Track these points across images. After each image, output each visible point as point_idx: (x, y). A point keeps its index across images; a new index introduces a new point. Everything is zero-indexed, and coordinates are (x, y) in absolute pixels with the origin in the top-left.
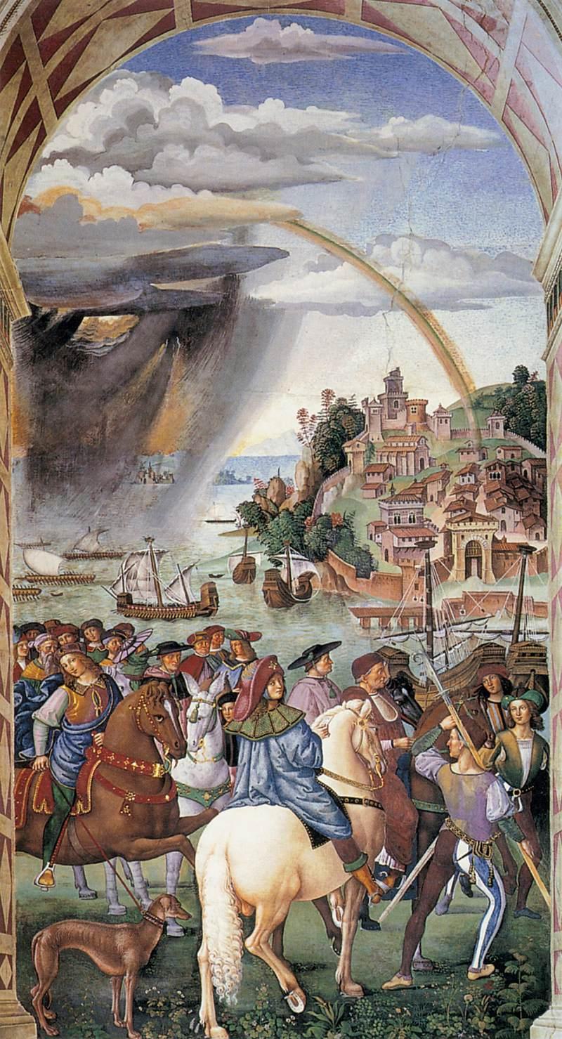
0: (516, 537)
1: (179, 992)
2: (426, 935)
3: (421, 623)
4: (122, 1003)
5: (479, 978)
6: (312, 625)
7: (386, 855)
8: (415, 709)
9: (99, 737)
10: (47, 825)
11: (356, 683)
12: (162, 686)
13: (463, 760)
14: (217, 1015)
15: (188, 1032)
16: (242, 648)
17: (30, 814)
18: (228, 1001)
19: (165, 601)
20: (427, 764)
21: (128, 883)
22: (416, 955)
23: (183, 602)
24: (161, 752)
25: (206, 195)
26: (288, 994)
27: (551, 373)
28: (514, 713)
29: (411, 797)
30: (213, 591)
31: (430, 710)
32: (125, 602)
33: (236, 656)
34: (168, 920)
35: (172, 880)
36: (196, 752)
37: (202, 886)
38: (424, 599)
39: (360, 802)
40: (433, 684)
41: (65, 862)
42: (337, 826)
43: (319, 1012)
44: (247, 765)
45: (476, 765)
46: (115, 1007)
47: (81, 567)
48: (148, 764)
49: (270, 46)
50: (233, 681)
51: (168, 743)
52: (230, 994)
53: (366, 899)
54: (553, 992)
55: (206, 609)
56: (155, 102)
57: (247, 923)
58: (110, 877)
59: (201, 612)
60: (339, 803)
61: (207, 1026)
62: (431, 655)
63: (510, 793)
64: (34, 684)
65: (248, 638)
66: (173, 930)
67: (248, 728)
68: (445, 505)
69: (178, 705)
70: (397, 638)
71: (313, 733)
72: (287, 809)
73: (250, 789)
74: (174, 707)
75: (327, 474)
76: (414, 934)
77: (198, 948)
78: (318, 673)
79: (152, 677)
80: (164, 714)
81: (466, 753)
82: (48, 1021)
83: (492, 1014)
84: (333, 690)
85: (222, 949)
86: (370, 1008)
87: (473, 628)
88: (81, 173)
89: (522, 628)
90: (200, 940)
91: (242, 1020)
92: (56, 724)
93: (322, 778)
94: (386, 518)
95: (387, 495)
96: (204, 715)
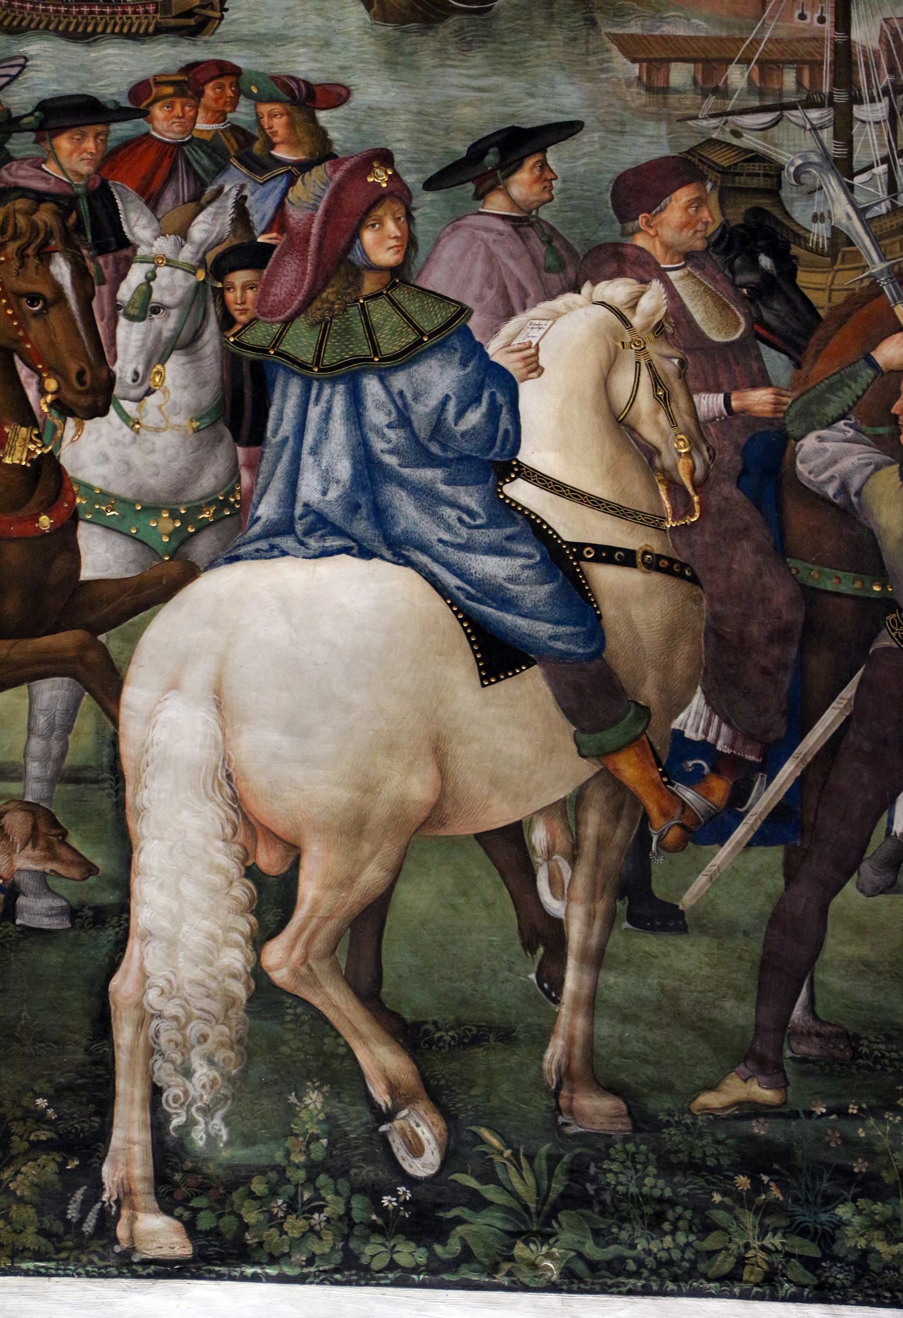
1: (41, 1102)
2: (826, 955)
3: (816, 80)
6: (495, 73)
7: (705, 712)
8: (794, 308)
11: (624, 234)
12: (45, 216)
15: (58, 1227)
16: (291, 125)
18: (198, 1137)
20: (834, 462)
22: (797, 1012)
24: (32, 393)
26: (389, 1116)
33: (273, 146)
34: (26, 881)
35: (45, 758)
36: (139, 400)
37: (138, 780)
38: (829, 18)
39: (627, 559)
40: (851, 244)
42: (558, 623)
43: (488, 1176)
44: (291, 443)
51: (58, 372)
52: (208, 1111)
53: (643, 838)
55: (188, 14)
59: (173, 22)
61: (125, 1213)
69: (90, 264)
70: (749, 120)
71: (495, 365)
72: (408, 573)
73: (299, 510)
74: (80, 273)
77: (113, 967)
78: (513, 202)
79: (17, 188)
80: (47, 292)
84: (554, 251)
86: (652, 1170)
91: (235, 1196)
96: (167, 300)
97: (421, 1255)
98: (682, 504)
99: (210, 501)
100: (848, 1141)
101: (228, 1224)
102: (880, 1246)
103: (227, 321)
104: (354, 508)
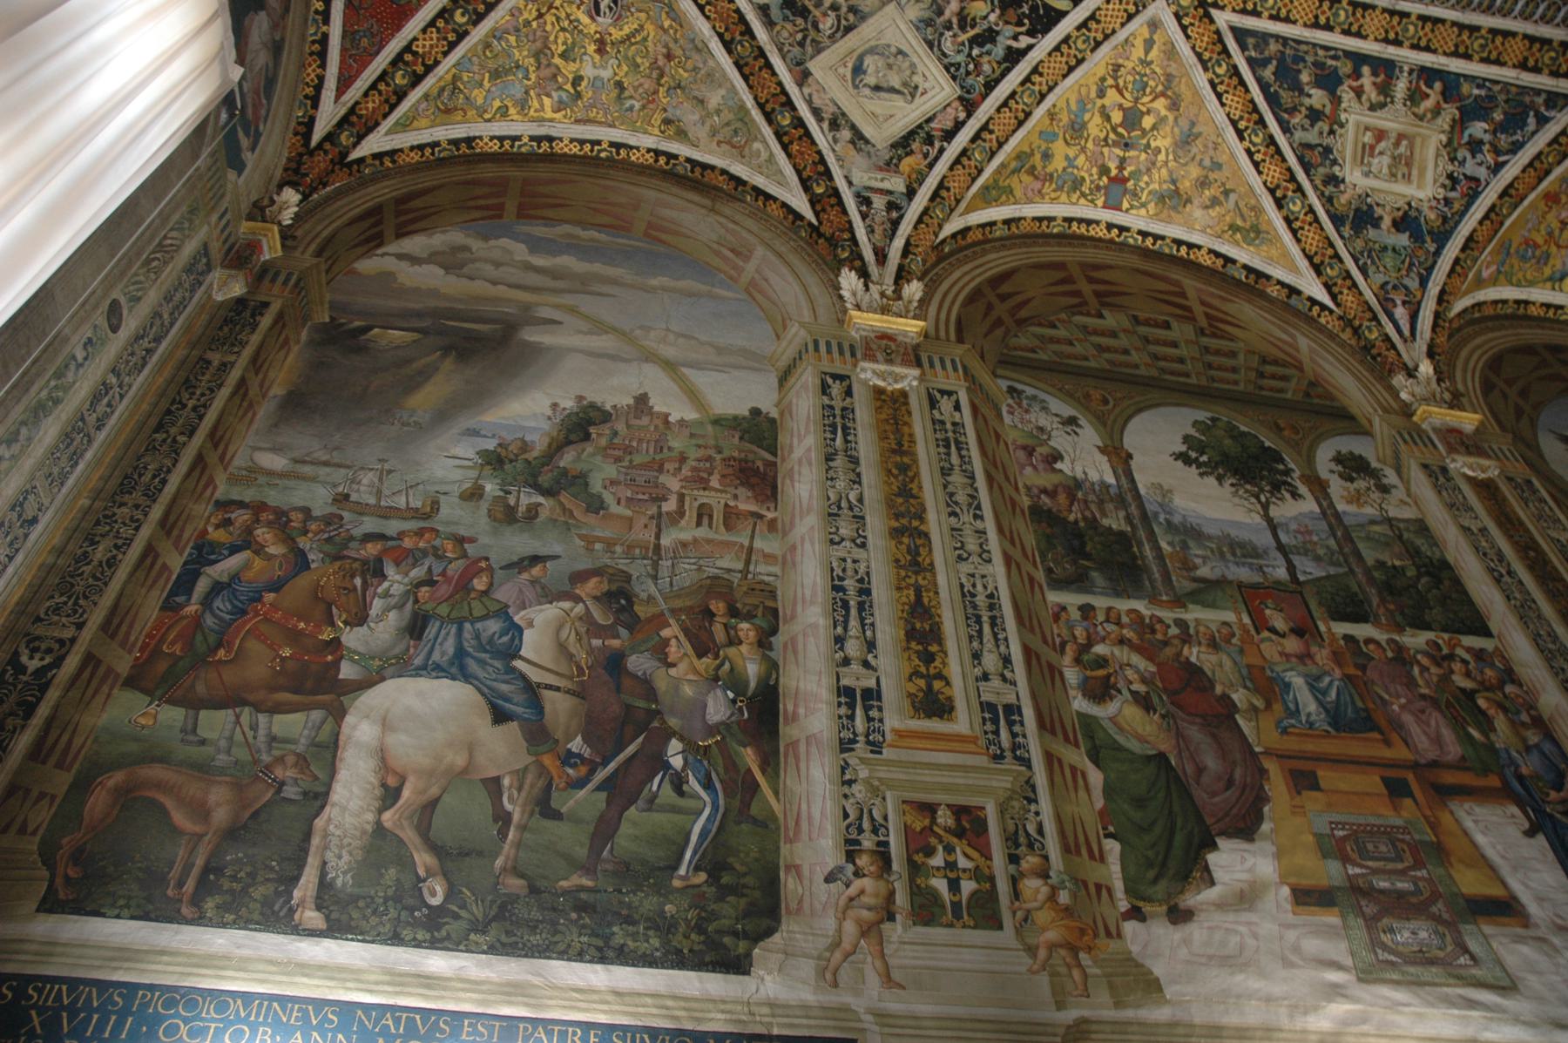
4: (188, 867)
5: (687, 887)
9: (269, 597)
12: (356, 565)
17: (156, 653)
18: (339, 882)
19: (383, 503)
21: (250, 734)
25: (500, 287)
26: (424, 881)
27: (782, 414)
28: (741, 634)
29: (618, 689)
31: (649, 620)
34: (289, 781)
39: (558, 689)
43: (463, 906)
45: (696, 672)
46: (174, 874)
47: (307, 469)
48: (318, 626)
49: (570, 236)
50: (437, 569)
51: (348, 612)
52: (345, 873)
53: (549, 786)
54: (783, 911)
56: (476, 245)
57: (390, 795)
58: (229, 727)
60: (532, 691)
62: (655, 578)
63: (734, 701)
65: (460, 541)
66: (290, 792)
67: (443, 610)
74: (365, 583)
75: (569, 443)
76: (605, 830)
77: (317, 815)
81: (686, 660)
83: (700, 929)
85: (349, 820)
88: (404, 265)
89: (752, 568)
90: (323, 807)
93: (518, 664)
94: (622, 478)
95: (626, 463)
97: (428, 936)
98: (581, 671)
99: (396, 657)
100: (621, 902)
101: (344, 918)
102: (630, 943)
103: (416, 601)
104: (452, 664)
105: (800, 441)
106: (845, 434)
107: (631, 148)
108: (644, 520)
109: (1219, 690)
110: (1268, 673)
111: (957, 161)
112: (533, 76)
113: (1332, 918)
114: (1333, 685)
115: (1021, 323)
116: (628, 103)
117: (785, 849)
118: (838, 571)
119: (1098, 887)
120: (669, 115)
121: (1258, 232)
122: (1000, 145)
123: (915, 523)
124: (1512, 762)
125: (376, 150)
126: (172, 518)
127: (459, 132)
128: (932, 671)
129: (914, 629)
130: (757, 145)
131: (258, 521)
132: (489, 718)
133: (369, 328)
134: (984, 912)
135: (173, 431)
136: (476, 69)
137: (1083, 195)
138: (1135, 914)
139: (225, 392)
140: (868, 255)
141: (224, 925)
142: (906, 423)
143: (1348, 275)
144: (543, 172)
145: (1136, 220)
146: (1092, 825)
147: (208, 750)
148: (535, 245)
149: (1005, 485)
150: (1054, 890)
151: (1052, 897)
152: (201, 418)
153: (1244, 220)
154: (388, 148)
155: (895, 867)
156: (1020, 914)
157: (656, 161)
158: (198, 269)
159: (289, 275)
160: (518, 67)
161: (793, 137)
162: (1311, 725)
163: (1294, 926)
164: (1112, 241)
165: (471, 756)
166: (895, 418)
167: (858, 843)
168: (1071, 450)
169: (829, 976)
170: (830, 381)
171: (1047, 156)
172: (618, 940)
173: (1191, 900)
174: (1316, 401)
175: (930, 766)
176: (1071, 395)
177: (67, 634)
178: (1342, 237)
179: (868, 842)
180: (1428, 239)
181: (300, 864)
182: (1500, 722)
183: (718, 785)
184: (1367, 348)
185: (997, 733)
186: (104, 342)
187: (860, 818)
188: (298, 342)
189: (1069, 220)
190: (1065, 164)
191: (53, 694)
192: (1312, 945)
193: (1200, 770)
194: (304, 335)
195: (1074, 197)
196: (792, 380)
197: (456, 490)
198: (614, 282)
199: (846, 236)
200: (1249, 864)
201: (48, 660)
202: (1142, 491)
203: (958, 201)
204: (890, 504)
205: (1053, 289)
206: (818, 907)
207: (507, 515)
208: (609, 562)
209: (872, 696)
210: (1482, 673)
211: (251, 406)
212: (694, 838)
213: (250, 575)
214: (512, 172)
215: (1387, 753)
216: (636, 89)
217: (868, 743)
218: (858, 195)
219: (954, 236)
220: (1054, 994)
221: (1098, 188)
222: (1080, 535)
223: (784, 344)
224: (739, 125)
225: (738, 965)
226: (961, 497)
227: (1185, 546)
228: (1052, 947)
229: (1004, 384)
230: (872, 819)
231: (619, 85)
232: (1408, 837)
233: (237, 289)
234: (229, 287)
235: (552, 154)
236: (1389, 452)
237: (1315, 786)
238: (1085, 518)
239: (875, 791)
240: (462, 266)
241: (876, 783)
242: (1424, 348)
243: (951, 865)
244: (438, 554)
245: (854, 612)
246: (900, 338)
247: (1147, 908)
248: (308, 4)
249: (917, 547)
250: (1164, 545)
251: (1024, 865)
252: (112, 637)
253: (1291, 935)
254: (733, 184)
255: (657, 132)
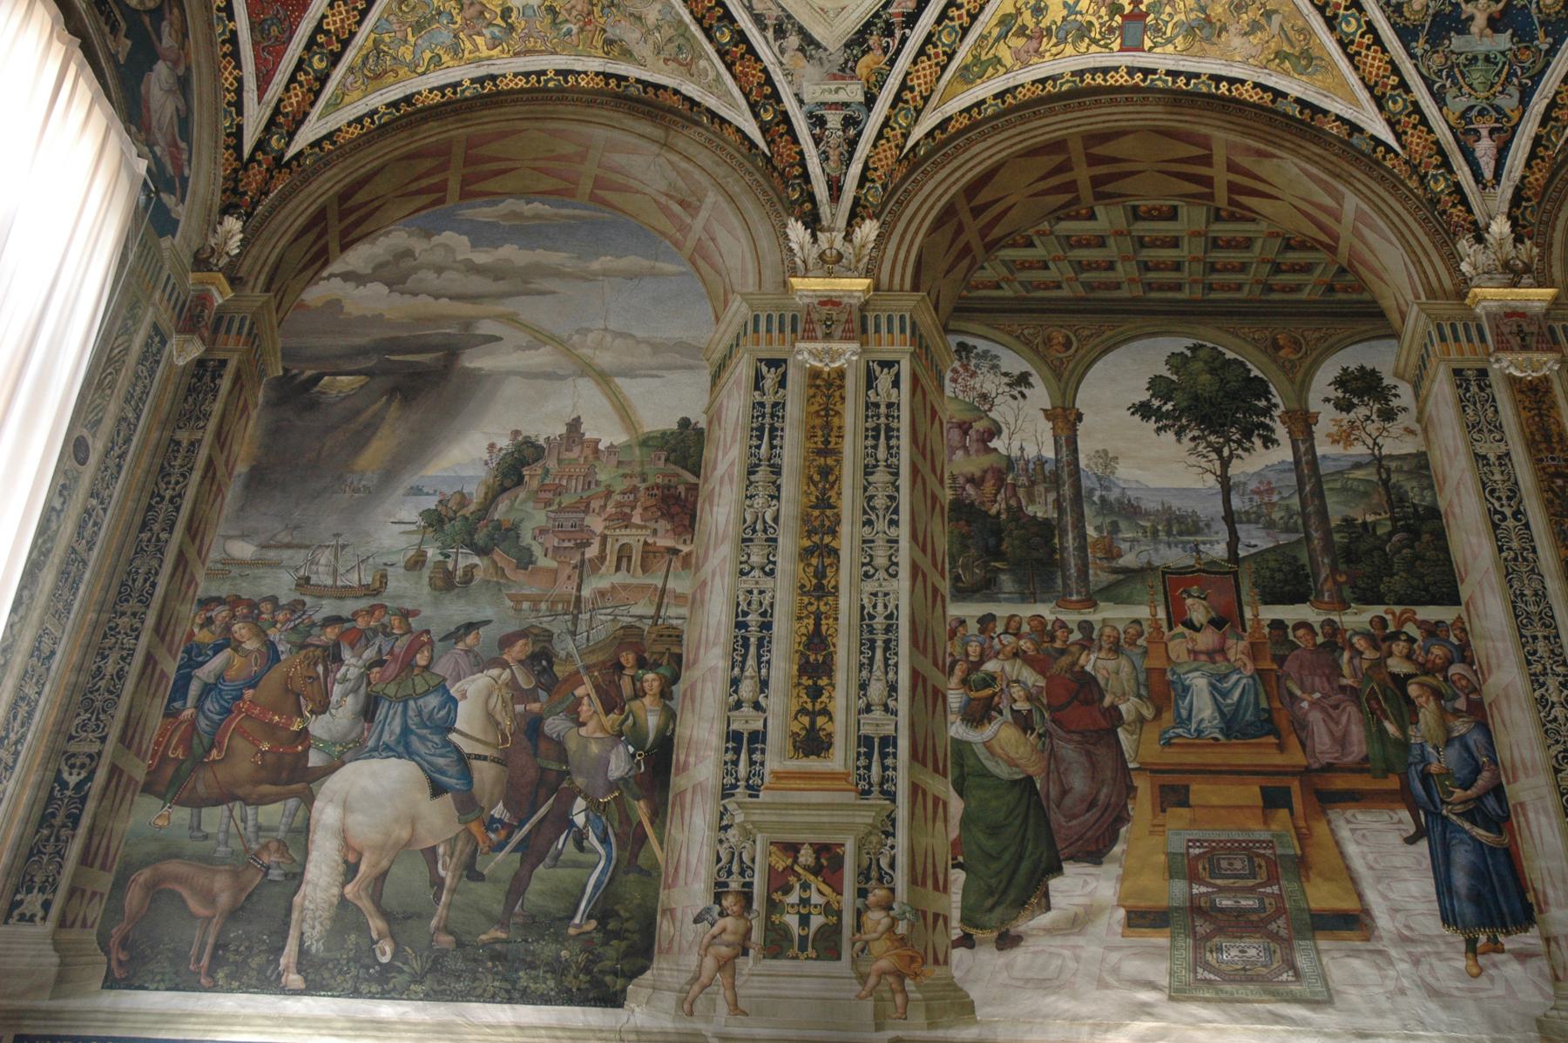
0: (665, 542)
2: (530, 888)
9: (249, 693)
10: (177, 770)
12: (318, 652)
13: (592, 725)
14: (299, 963)
17: (164, 757)
18: (314, 949)
19: (339, 583)
21: (241, 826)
23: (355, 583)
27: (710, 423)
29: (536, 755)
30: (384, 576)
31: (566, 680)
32: (304, 583)
39: (485, 758)
41: (182, 804)
45: (603, 729)
47: (271, 554)
48: (290, 718)
50: (386, 649)
51: (313, 700)
56: (419, 245)
57: (350, 870)
58: (225, 820)
60: (463, 760)
62: (574, 634)
63: (633, 756)
64: (200, 648)
65: (405, 614)
66: (275, 874)
67: (391, 690)
68: (604, 516)
74: (326, 669)
75: (504, 490)
76: (517, 887)
81: (595, 718)
82: (120, 962)
87: (617, 612)
88: (350, 286)
90: (299, 886)
92: (212, 681)
93: (453, 737)
95: (555, 507)
98: (505, 740)
99: (353, 741)
101: (318, 978)
103: (369, 683)
104: (398, 742)
105: (725, 454)
106: (772, 438)
107: (579, 73)
108: (568, 570)
109: (1107, 701)
110: (1169, 676)
111: (921, 52)
112: (458, 19)
113: (1161, 940)
114: (1238, 686)
115: (991, 247)
116: (565, 28)
117: (663, 895)
118: (744, 606)
119: (936, 916)
120: (609, 35)
121: (1310, 59)
122: (973, 18)
123: (827, 539)
124: (1424, 759)
125: (312, 139)
126: (164, 622)
127: (395, 93)
128: (818, 706)
129: (807, 662)
130: (703, 63)
131: (234, 616)
132: (428, 792)
133: (317, 379)
134: (827, 944)
135: (156, 527)
136: (395, 27)
137: (1094, 41)
138: (967, 941)
139: (196, 477)
140: (821, 190)
141: (231, 991)
142: (837, 413)
143: (1416, 108)
144: (488, 122)
145: (1163, 58)
146: (943, 854)
147: (210, 843)
148: (481, 235)
149: (930, 478)
150: (894, 921)
151: (891, 928)
152: (178, 509)
153: (1292, 46)
154: (324, 132)
155: (755, 906)
156: (858, 945)
157: (607, 84)
158: (151, 356)
159: (243, 320)
160: (440, 13)
161: (737, 54)
162: (1199, 732)
163: (1118, 948)
164: (1136, 89)
165: (413, 830)
166: (826, 409)
167: (726, 885)
168: (1011, 421)
169: (687, 1007)
170: (764, 369)
171: (1038, 11)
172: (523, 983)
173: (1023, 925)
174: (1341, 296)
175: (800, 806)
176: (1028, 343)
177: (95, 748)
178: (1412, 56)
179: (734, 885)
180: (1541, 34)
181: (285, 938)
182: (1428, 713)
183: (613, 839)
184: (1434, 201)
185: (868, 768)
186: (76, 479)
187: (731, 862)
188: (256, 406)
189: (1080, 73)
190: (1065, 12)
191: (91, 806)
192: (1133, 967)
193: (1064, 792)
194: (261, 395)
195: (1083, 47)
196: (725, 375)
197: (401, 559)
198: (556, 273)
199: (797, 171)
200: (1089, 888)
201: (83, 775)
202: (1083, 463)
203: (926, 99)
204: (805, 519)
205: (1042, 185)
206: (685, 945)
207: (447, 582)
208: (534, 621)
209: (758, 737)
210: (1428, 652)
211: (219, 489)
212: (589, 889)
213: (232, 673)
214: (456, 131)
215: (1278, 759)
216: (569, 11)
217: (748, 787)
218: (810, 115)
219: (930, 134)
220: (876, 1015)
221: (1111, 30)
222: (997, 532)
223: (723, 327)
224: (681, 41)
225: (613, 1000)
226: (880, 502)
227: (1115, 528)
228: (882, 974)
229: (953, 340)
230: (741, 861)
231: (551, 9)
232: (1268, 852)
233: (195, 350)
234: (185, 352)
235: (499, 93)
236: (1414, 359)
237: (1184, 803)
238: (1009, 508)
239: (748, 835)
240: (403, 279)
241: (750, 827)
242: (1509, 194)
243: (805, 902)
244: (386, 631)
245: (753, 650)
246: (845, 300)
247: (978, 935)
248: (207, 7)
249: (824, 567)
250: (1091, 532)
251: (871, 898)
252: (129, 747)
253: (1114, 957)
254: (687, 105)
255: (600, 52)
